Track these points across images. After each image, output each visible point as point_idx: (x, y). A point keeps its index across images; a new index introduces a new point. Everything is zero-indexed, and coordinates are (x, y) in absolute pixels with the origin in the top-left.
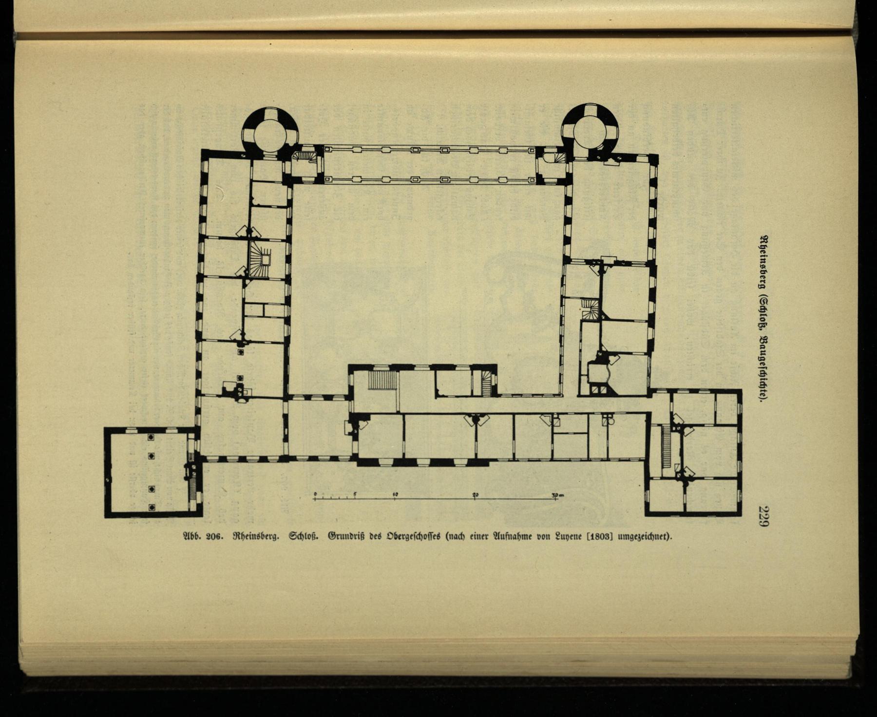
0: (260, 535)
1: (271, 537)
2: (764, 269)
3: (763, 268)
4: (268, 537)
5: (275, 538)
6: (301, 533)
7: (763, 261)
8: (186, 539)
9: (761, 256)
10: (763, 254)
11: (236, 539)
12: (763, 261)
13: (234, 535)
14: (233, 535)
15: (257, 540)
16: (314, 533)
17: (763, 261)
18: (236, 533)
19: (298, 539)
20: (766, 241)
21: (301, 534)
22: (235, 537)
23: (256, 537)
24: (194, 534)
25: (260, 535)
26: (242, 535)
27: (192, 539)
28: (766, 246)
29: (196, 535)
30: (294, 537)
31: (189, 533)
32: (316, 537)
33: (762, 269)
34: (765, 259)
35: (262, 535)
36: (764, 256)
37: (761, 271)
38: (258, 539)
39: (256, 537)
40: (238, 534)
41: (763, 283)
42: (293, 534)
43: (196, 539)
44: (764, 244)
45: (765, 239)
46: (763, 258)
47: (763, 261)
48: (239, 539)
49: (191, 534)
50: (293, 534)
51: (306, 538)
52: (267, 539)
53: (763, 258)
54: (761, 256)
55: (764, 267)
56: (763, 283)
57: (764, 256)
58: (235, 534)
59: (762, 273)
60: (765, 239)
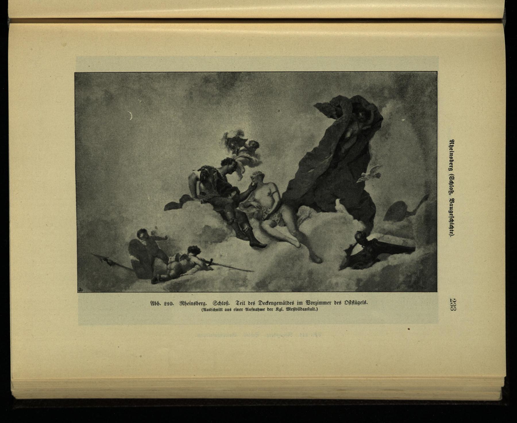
0: (196, 303)
2: (452, 159)
3: (451, 159)
4: (201, 304)
5: (205, 304)
6: (220, 302)
7: (451, 155)
8: (152, 305)
9: (450, 152)
10: (451, 151)
11: (182, 305)
12: (451, 154)
13: (180, 303)
14: (179, 303)
15: (194, 305)
16: (227, 301)
17: (451, 154)
18: (182, 302)
19: (218, 305)
20: (453, 143)
21: (220, 302)
22: (181, 304)
23: (194, 304)
24: (157, 302)
25: (196, 303)
26: (185, 303)
27: (155, 305)
28: (453, 146)
29: (158, 303)
30: (216, 304)
31: (153, 302)
32: (229, 304)
33: (451, 159)
34: (452, 154)
35: (197, 303)
36: (452, 152)
37: (450, 160)
38: (195, 305)
39: (194, 304)
40: (183, 302)
41: (451, 167)
42: (215, 302)
43: (158, 305)
44: (452, 144)
45: (452, 142)
46: (451, 153)
47: (451, 155)
48: (183, 305)
49: (155, 302)
50: (215, 302)
51: (223, 305)
52: (200, 305)
53: (451, 153)
54: (450, 152)
55: (451, 158)
56: (451, 167)
57: (452, 152)
58: (181, 302)
59: (450, 162)
60: (452, 142)
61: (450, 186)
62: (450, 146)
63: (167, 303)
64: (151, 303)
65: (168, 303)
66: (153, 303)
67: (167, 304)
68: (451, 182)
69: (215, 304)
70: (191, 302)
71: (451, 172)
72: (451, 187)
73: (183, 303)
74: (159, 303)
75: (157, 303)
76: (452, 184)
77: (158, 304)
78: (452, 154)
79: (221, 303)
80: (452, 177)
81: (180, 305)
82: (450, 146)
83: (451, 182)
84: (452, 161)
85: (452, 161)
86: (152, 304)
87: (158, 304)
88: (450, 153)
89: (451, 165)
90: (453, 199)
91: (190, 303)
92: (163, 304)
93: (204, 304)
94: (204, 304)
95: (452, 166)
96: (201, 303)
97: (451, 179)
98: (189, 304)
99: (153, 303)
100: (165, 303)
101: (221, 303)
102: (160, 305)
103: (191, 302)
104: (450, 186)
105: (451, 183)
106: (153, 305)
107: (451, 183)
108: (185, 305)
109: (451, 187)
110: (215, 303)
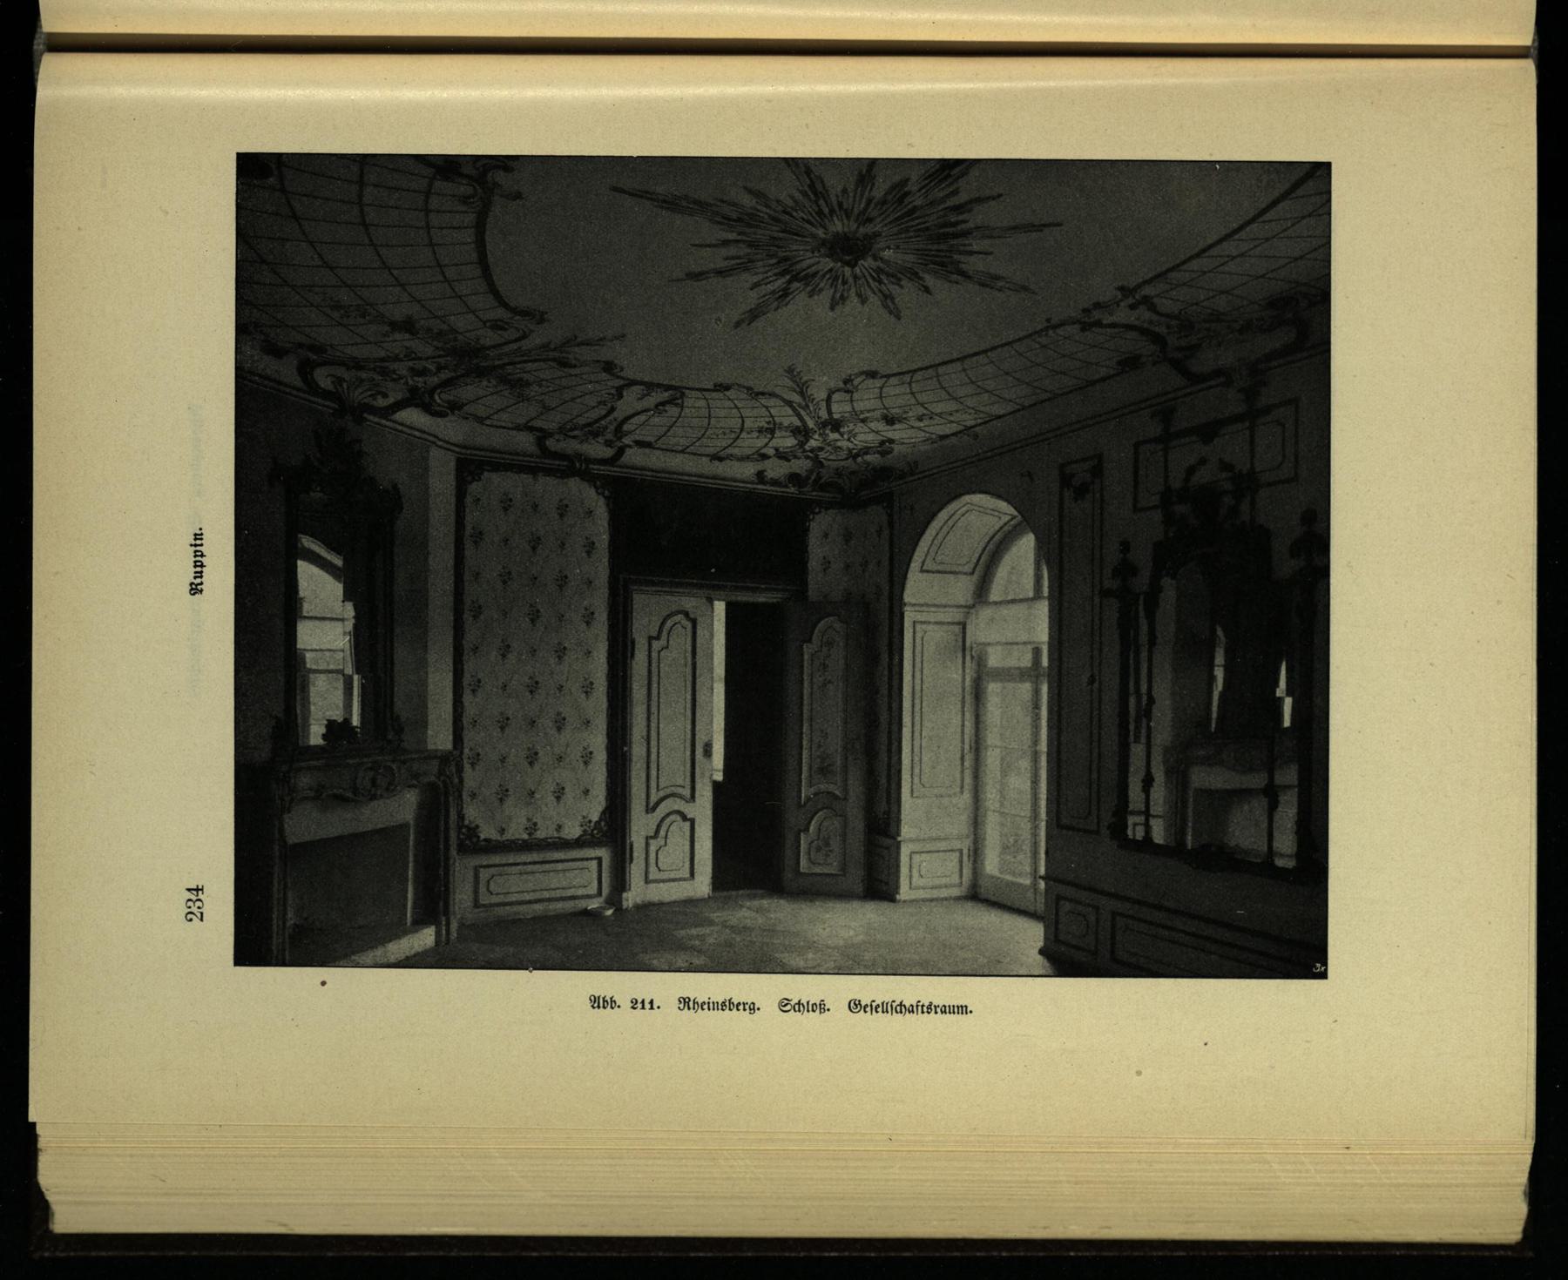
0: (727, 1004)
1: (747, 1007)
4: (741, 1007)
8: (594, 1007)
18: (684, 999)
22: (682, 1006)
23: (720, 1007)
25: (727, 1004)
26: (694, 1003)
27: (604, 1007)
29: (611, 1002)
30: (788, 1007)
38: (723, 1010)
39: (720, 1007)
40: (687, 1000)
42: (786, 1002)
43: (612, 1008)
46: (198, 542)
48: (689, 1008)
50: (786, 1002)
52: (738, 1010)
53: (198, 542)
57: (196, 545)
58: (681, 1000)
63: (640, 1001)
64: (591, 1000)
65: (643, 1002)
66: (598, 1002)
67: (640, 1006)
69: (784, 1009)
70: (711, 1001)
73: (685, 1002)
74: (615, 1001)
75: (609, 1001)
77: (611, 1003)
79: (804, 1006)
81: (679, 1008)
86: (596, 1005)
87: (611, 1003)
88: (203, 542)
91: (709, 1003)
92: (626, 1004)
93: (752, 1007)
94: (752, 1007)
96: (744, 1004)
98: (706, 1007)
99: (598, 1002)
100: (632, 1002)
101: (804, 1006)
102: (619, 1007)
103: (711, 1001)
106: (599, 1007)
108: (694, 1009)
110: (784, 1006)
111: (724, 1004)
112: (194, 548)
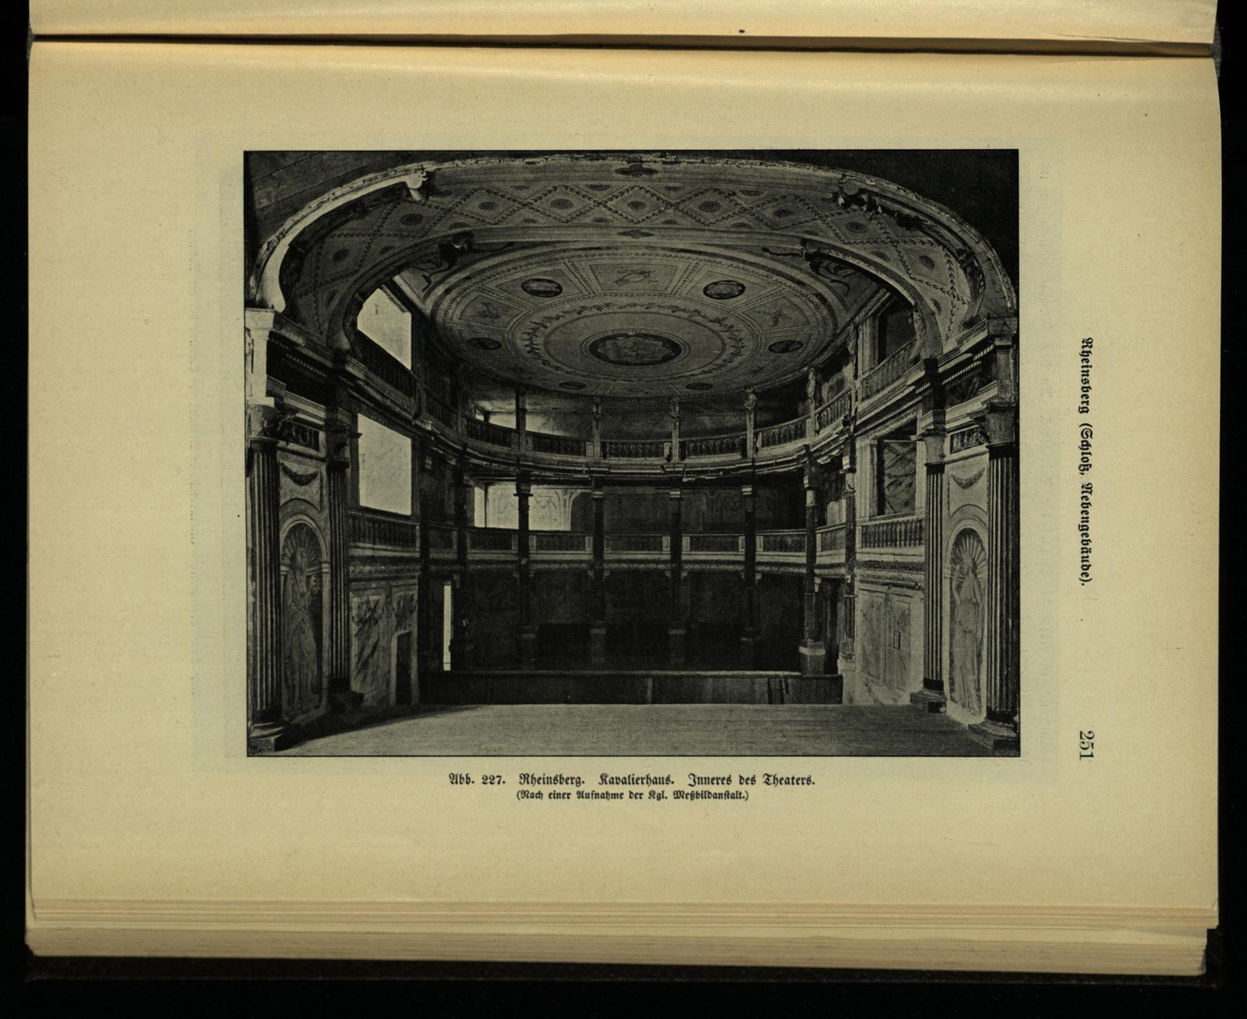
0: (558, 778)
2: (1087, 385)
9: (1083, 367)
10: (1085, 364)
12: (1085, 373)
17: (1085, 373)
25: (558, 778)
34: (1088, 371)
36: (1087, 366)
41: (1085, 405)
46: (1085, 369)
53: (1085, 369)
54: (1083, 367)
55: (1086, 381)
56: (1085, 405)
57: (1087, 366)
61: (1083, 454)
62: (1083, 352)
68: (1085, 443)
71: (1085, 418)
72: (1085, 456)
76: (1087, 449)
78: (1088, 371)
80: (1087, 432)
82: (1083, 352)
83: (1085, 443)
84: (1086, 389)
85: (1086, 389)
89: (1085, 400)
90: (1089, 484)
95: (1087, 402)
97: (1085, 436)
104: (1083, 454)
105: (1085, 445)
107: (1085, 445)
109: (1085, 456)
111: (556, 779)
112: (1089, 364)
